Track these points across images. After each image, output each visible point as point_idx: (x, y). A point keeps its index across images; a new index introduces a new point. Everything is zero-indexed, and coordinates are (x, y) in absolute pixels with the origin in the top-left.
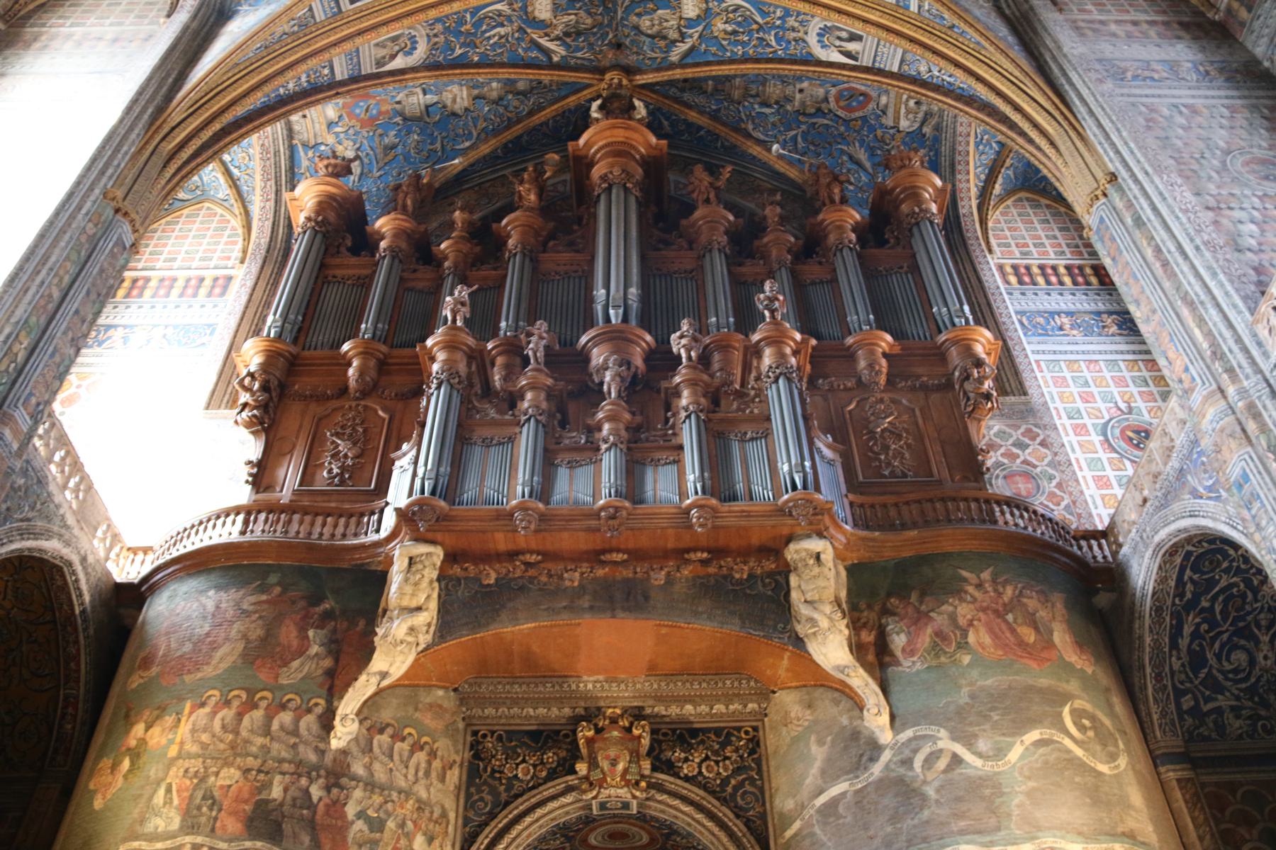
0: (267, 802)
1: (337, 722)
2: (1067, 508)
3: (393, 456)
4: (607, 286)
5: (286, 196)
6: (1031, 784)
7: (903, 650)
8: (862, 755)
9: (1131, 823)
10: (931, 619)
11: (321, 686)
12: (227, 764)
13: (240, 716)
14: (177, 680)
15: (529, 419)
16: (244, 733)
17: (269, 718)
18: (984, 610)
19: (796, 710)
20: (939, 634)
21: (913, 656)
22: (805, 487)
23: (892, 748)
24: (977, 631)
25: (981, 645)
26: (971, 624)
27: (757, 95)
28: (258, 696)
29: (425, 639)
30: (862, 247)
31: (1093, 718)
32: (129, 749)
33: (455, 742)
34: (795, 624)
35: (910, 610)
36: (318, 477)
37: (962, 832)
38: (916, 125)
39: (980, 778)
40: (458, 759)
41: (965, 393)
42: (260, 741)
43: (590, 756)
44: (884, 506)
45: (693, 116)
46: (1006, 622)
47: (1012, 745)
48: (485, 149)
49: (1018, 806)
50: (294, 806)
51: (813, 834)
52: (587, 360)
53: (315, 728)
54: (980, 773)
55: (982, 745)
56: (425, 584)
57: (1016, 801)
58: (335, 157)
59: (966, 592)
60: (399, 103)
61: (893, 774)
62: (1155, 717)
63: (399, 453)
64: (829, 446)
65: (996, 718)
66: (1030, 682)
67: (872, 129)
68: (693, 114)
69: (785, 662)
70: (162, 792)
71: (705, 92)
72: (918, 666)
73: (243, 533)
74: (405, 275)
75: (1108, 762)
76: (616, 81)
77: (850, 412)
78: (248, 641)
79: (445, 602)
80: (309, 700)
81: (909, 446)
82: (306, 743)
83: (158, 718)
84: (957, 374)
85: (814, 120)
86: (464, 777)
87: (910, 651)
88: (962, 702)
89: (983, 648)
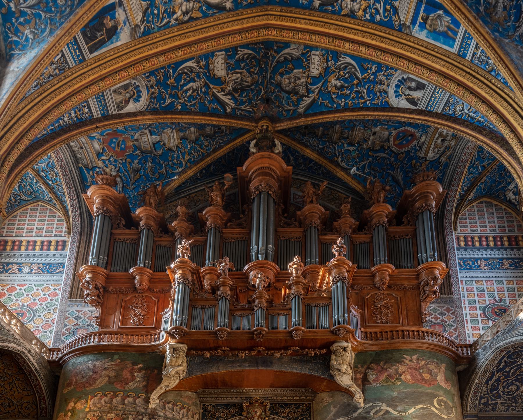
1: (151, 400)
3: (161, 314)
4: (258, 244)
5: (83, 196)
7: (373, 380)
11: (143, 390)
12: (109, 412)
13: (111, 399)
14: (83, 389)
15: (222, 298)
18: (410, 368)
25: (407, 379)
27: (348, 138)
30: (389, 226)
33: (197, 408)
34: (331, 371)
35: (379, 368)
36: (128, 323)
38: (438, 156)
40: (198, 412)
41: (424, 291)
42: (121, 406)
43: (247, 411)
44: (376, 333)
45: (308, 153)
46: (419, 373)
48: (190, 173)
52: (248, 277)
53: (142, 402)
55: (399, 408)
56: (181, 357)
58: (106, 174)
59: (404, 362)
60: (137, 140)
63: (164, 312)
64: (355, 310)
67: (411, 159)
68: (308, 151)
71: (317, 136)
72: (379, 385)
74: (156, 239)
76: (265, 127)
77: (367, 299)
78: (109, 377)
79: (189, 365)
81: (391, 312)
82: (139, 406)
83: (78, 401)
84: (422, 283)
85: (378, 154)
86: (201, 417)
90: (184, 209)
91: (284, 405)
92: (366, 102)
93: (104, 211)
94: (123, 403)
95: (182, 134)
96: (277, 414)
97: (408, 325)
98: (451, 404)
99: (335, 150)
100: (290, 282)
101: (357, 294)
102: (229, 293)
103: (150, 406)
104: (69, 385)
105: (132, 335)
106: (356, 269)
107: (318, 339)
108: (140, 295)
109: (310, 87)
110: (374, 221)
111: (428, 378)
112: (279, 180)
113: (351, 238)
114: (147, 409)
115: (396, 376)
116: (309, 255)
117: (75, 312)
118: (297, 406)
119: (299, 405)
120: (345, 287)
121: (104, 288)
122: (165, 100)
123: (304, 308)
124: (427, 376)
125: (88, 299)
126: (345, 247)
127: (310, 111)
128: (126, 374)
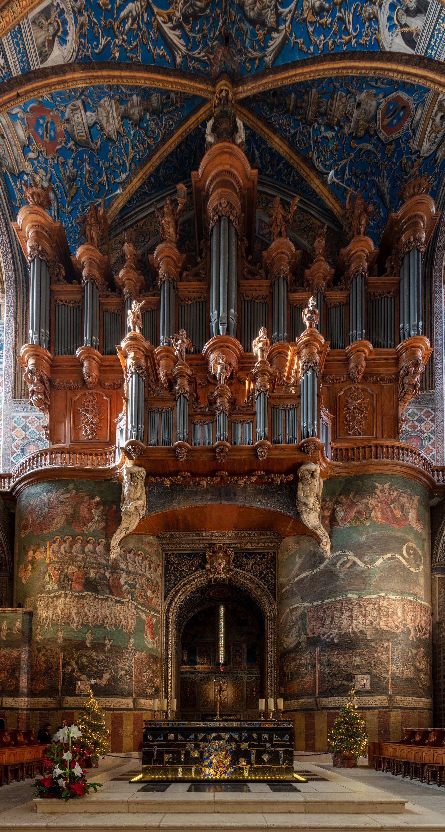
0: (89, 578)
1: (111, 548)
2: (433, 457)
3: (115, 421)
5: (12, 225)
7: (342, 519)
9: (417, 590)
10: (357, 505)
11: (102, 534)
12: (70, 565)
13: (71, 546)
14: (41, 533)
16: (74, 553)
17: (83, 547)
18: (381, 502)
19: (292, 545)
20: (359, 513)
22: (313, 436)
25: (376, 517)
26: (374, 508)
28: (77, 538)
29: (143, 513)
30: (369, 276)
32: (29, 561)
34: (297, 506)
36: (80, 435)
42: (81, 556)
46: (390, 508)
47: (378, 559)
50: (100, 580)
53: (103, 551)
59: (375, 493)
69: (291, 524)
70: (47, 576)
71: (288, 111)
72: (347, 526)
73: (51, 464)
77: (339, 397)
78: (67, 515)
80: (98, 540)
81: (365, 417)
82: (100, 557)
83: (37, 548)
87: (344, 520)
89: (377, 519)
90: (131, 248)
91: (249, 554)
92: (350, 40)
93: (39, 252)
94: (84, 552)
95: (122, 108)
96: (241, 566)
97: (382, 437)
98: (420, 552)
99: (310, 137)
100: (255, 371)
101: (328, 389)
102: (187, 388)
103: (111, 556)
104: (26, 526)
105: (85, 454)
106: (329, 350)
107: (284, 458)
108: (90, 391)
109: (281, 10)
110: (353, 266)
111: (399, 516)
112: (242, 197)
113: (324, 296)
114: (108, 560)
115: (366, 513)
116: (276, 326)
117: (22, 419)
118: (262, 555)
119: (264, 555)
120: (316, 379)
121: (50, 381)
122: (97, 39)
123: (270, 413)
124: (398, 514)
125: (34, 398)
126: (317, 311)
127: (280, 62)
128: (83, 511)
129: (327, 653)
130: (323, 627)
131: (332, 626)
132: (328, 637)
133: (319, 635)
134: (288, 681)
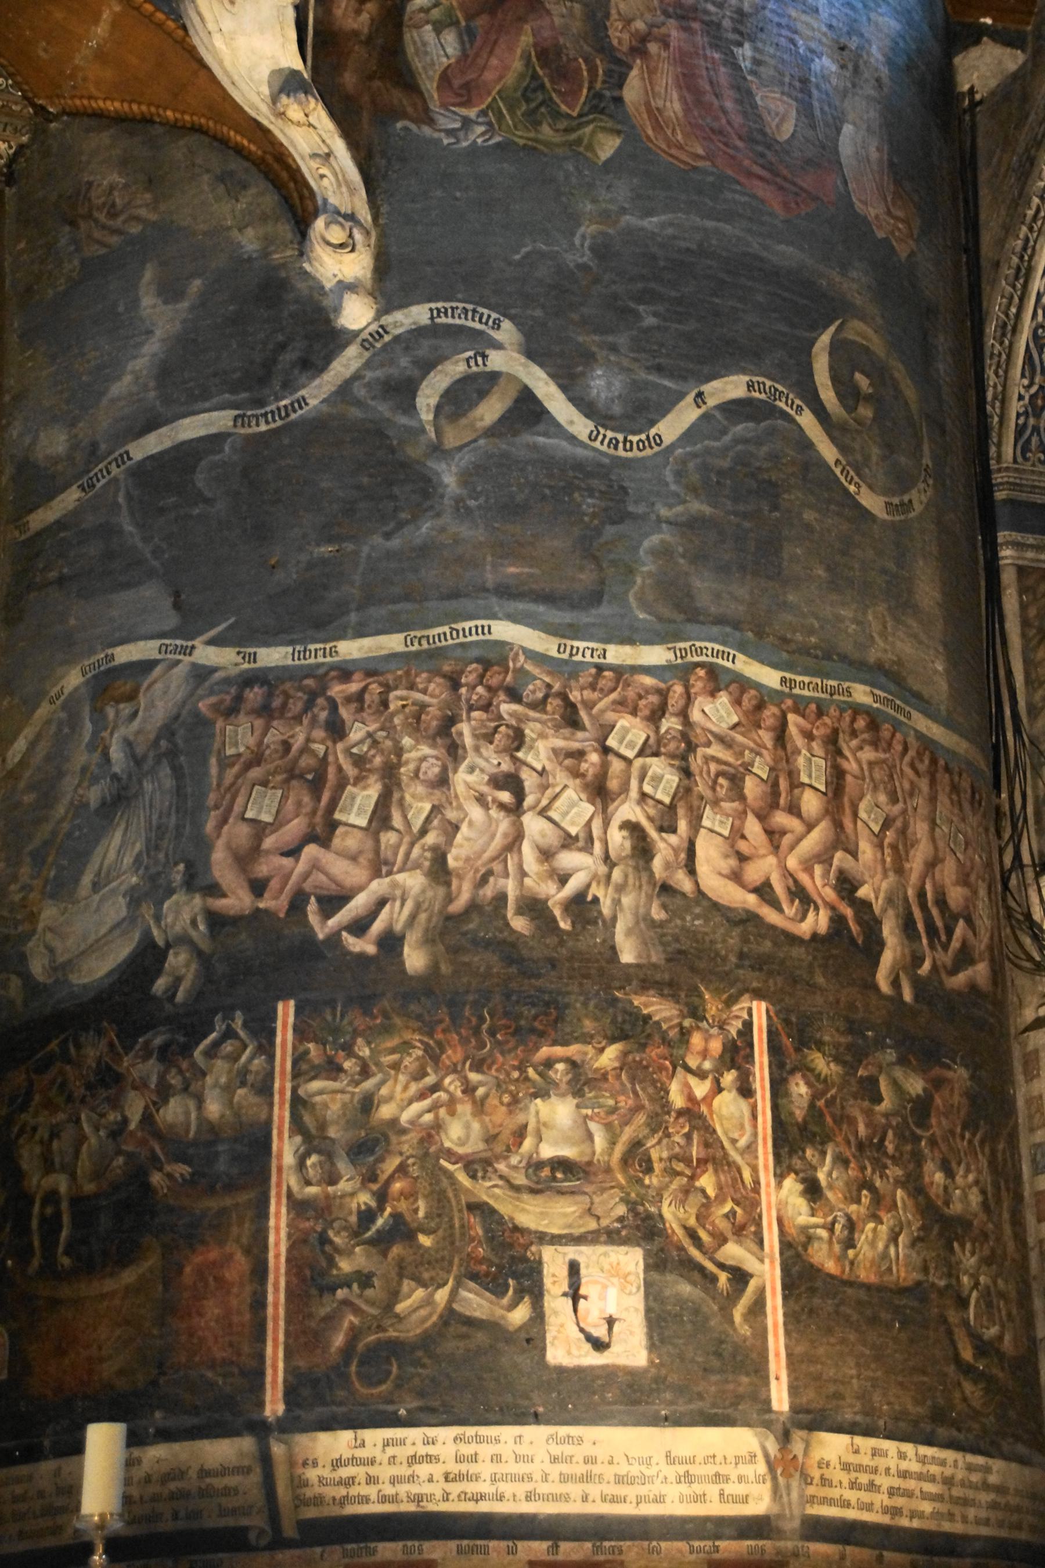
6: (698, 506)
7: (445, 79)
8: (282, 347)
21: (467, 103)
23: (365, 345)
24: (652, 72)
25: (655, 115)
26: (639, 49)
31: (879, 373)
37: (507, 592)
39: (579, 466)
49: (653, 552)
51: (108, 531)
54: (580, 452)
57: (655, 539)
61: (355, 413)
62: (1015, 407)
65: (650, 321)
66: (755, 246)
72: (477, 134)
75: (886, 492)
88: (571, 259)
89: (658, 127)
111: (787, 130)
115: (593, 70)
129: (349, 1049)
130: (325, 842)
131: (389, 838)
132: (359, 927)
133: (298, 903)
134: (50, 1270)
